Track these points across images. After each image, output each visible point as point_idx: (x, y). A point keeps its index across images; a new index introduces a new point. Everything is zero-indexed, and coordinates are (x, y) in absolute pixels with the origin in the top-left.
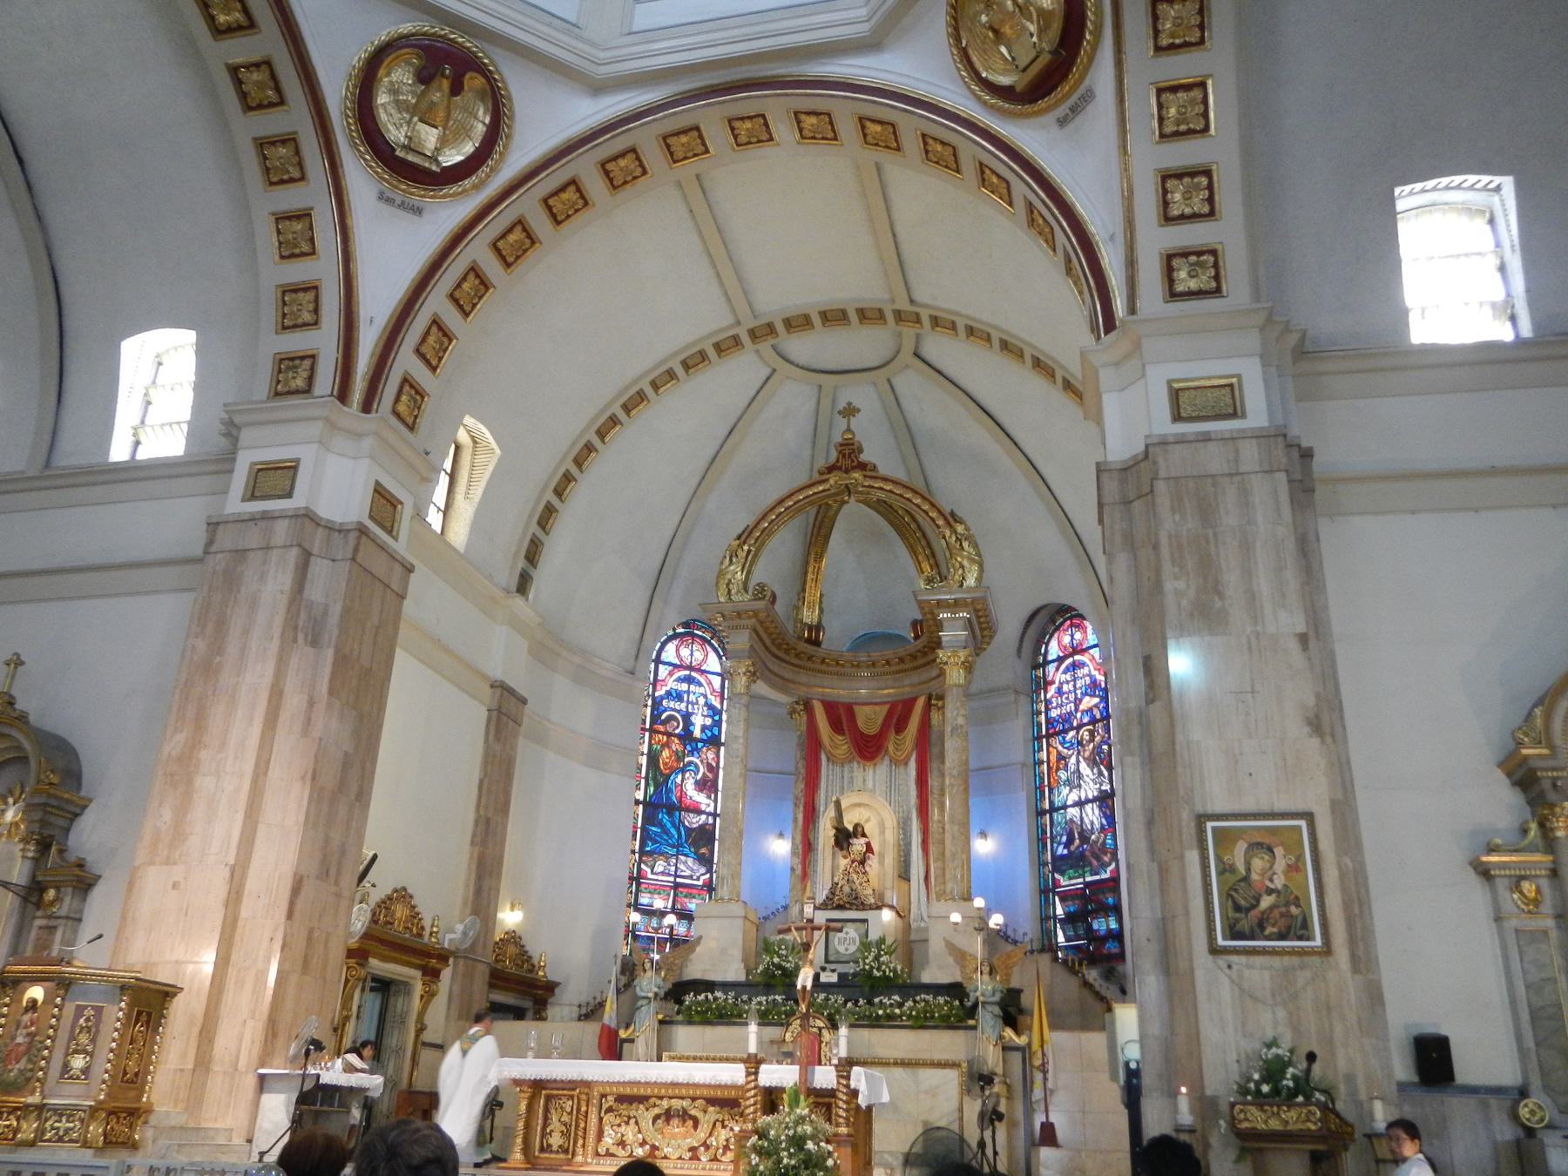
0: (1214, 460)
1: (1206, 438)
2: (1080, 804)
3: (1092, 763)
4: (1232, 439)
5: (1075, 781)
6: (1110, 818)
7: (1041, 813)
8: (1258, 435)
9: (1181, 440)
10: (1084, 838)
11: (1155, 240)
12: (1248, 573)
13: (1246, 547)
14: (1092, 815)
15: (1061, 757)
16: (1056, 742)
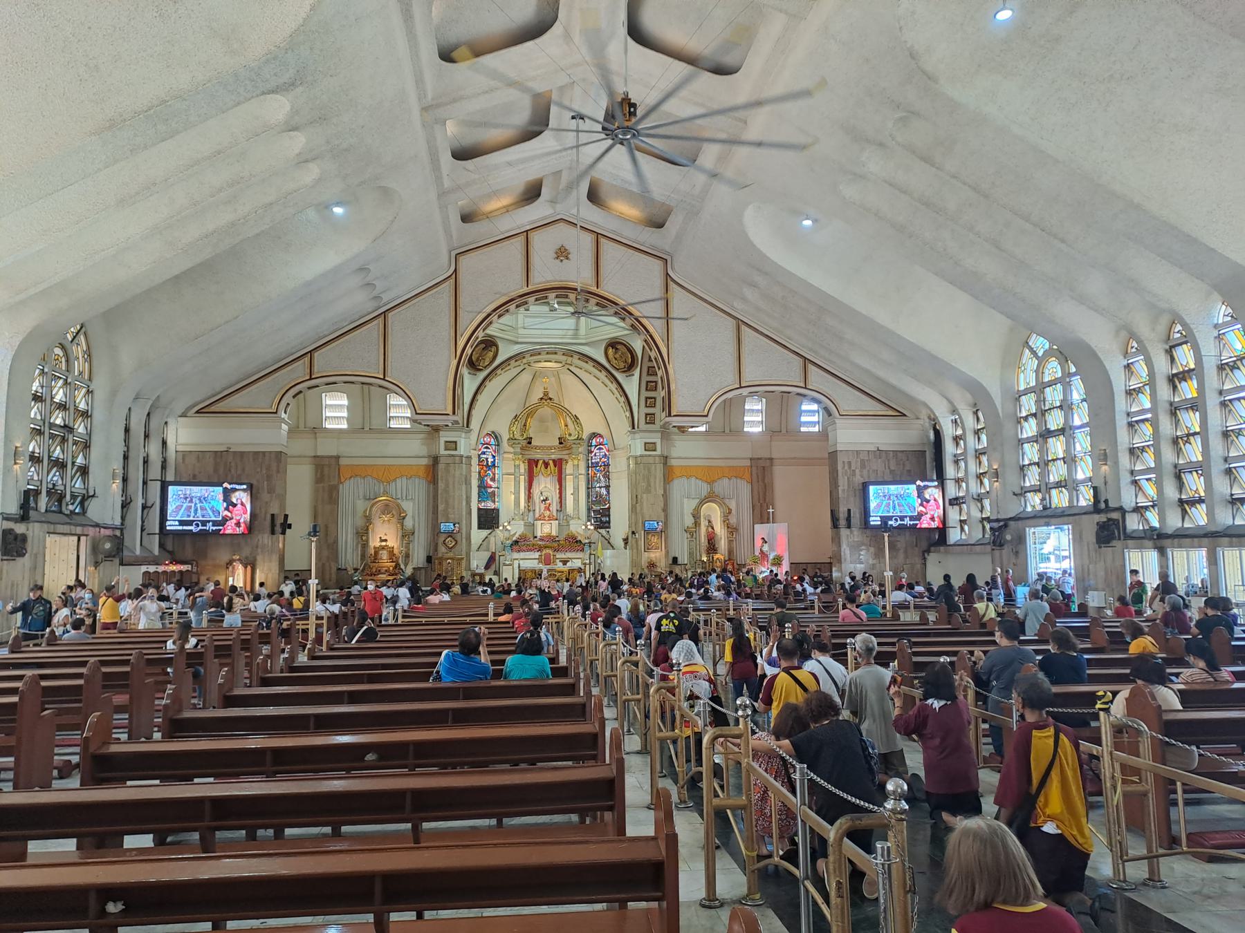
0: (651, 460)
1: (650, 456)
2: (600, 487)
3: (604, 477)
4: (655, 456)
5: (599, 481)
6: (608, 492)
7: (588, 488)
8: (659, 456)
9: (646, 456)
10: (601, 497)
11: (645, 410)
12: (655, 482)
13: (655, 478)
14: (604, 491)
15: (595, 474)
16: (593, 469)
